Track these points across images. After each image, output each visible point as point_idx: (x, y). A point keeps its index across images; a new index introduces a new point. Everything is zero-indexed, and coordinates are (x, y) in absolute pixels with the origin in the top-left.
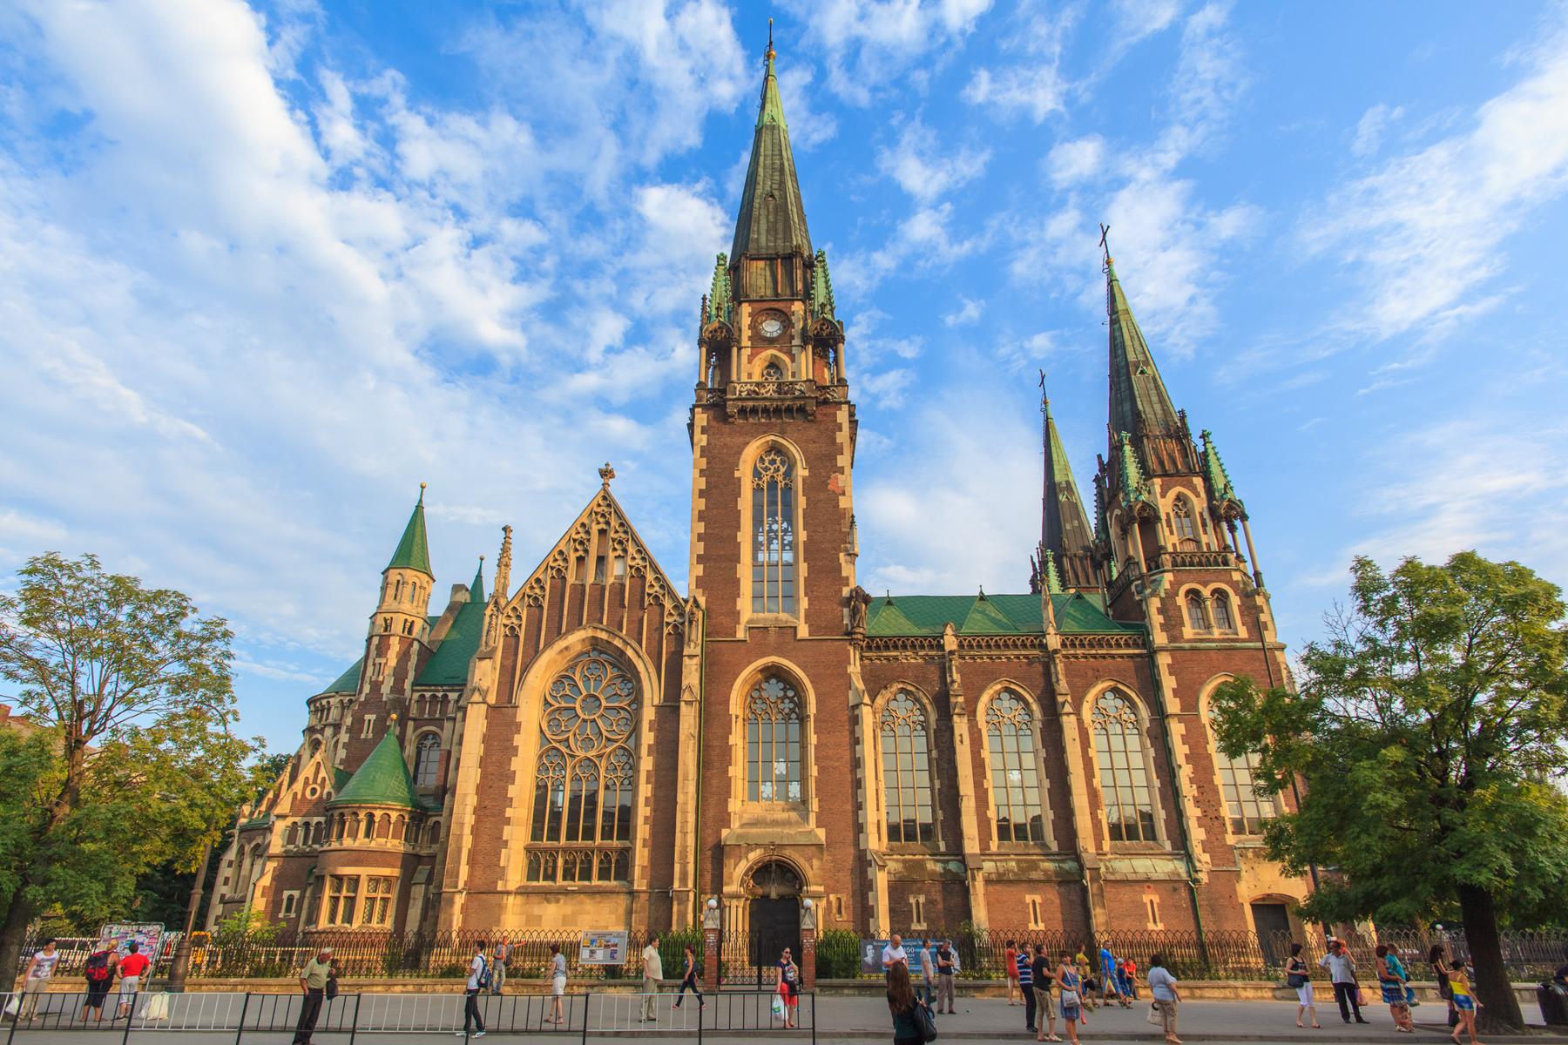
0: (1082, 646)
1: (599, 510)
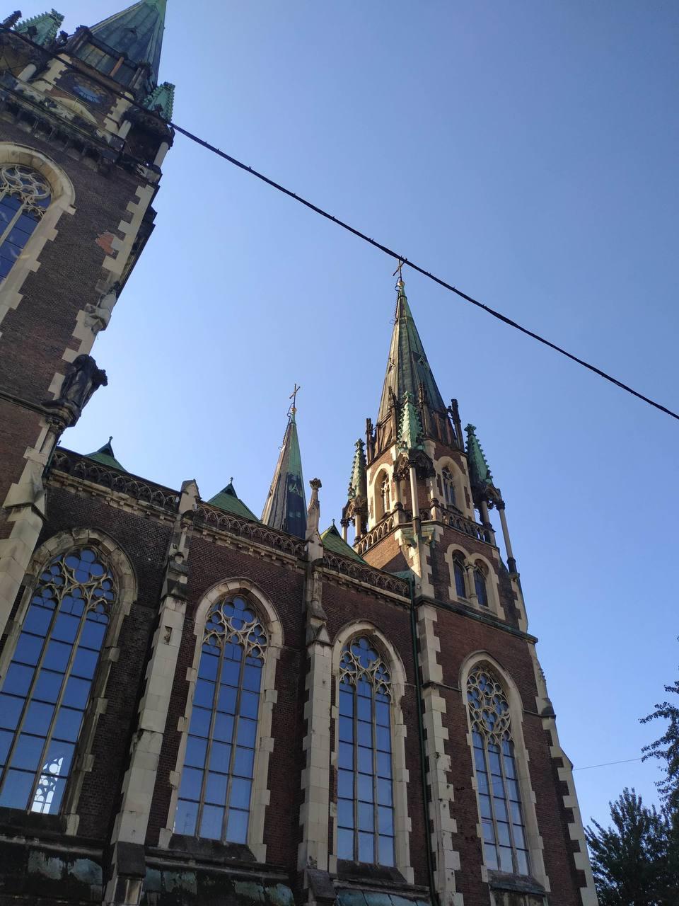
0: (343, 570)
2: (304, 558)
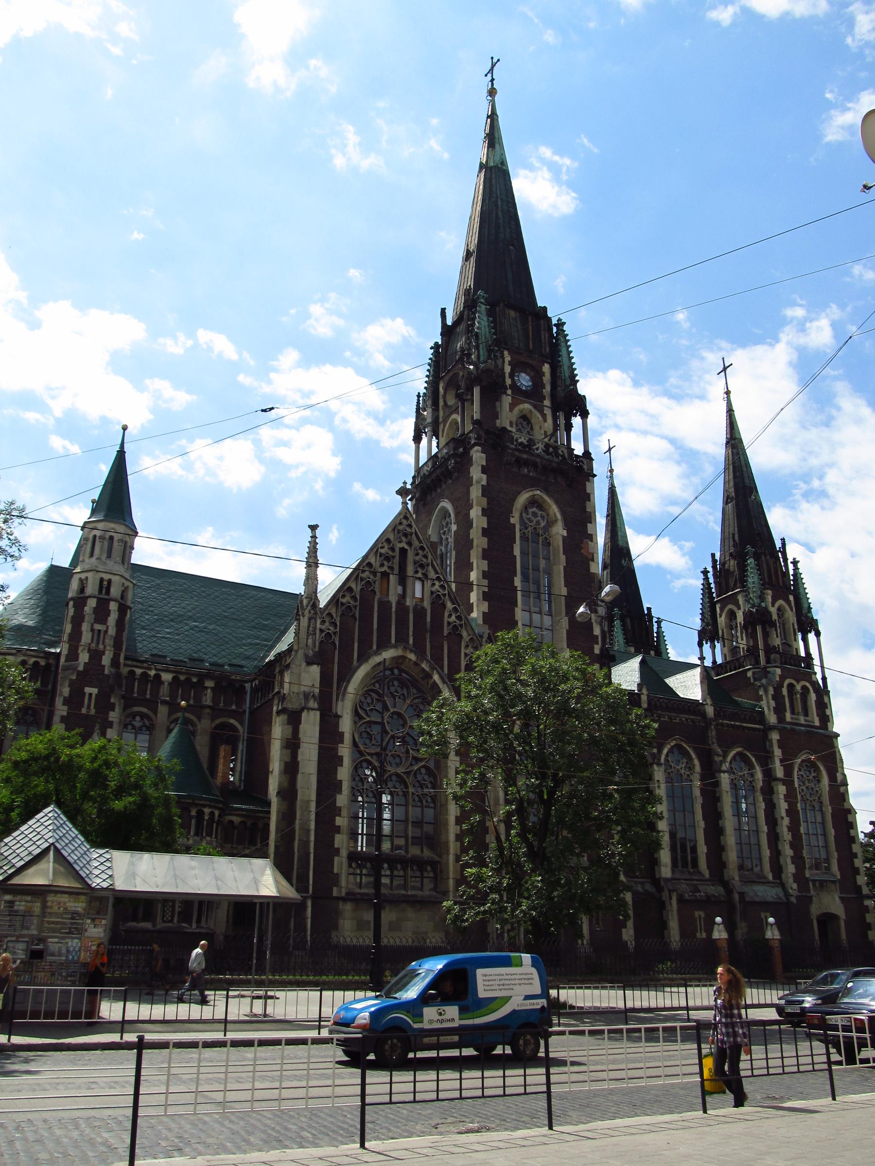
1: (401, 528)
2: (703, 714)
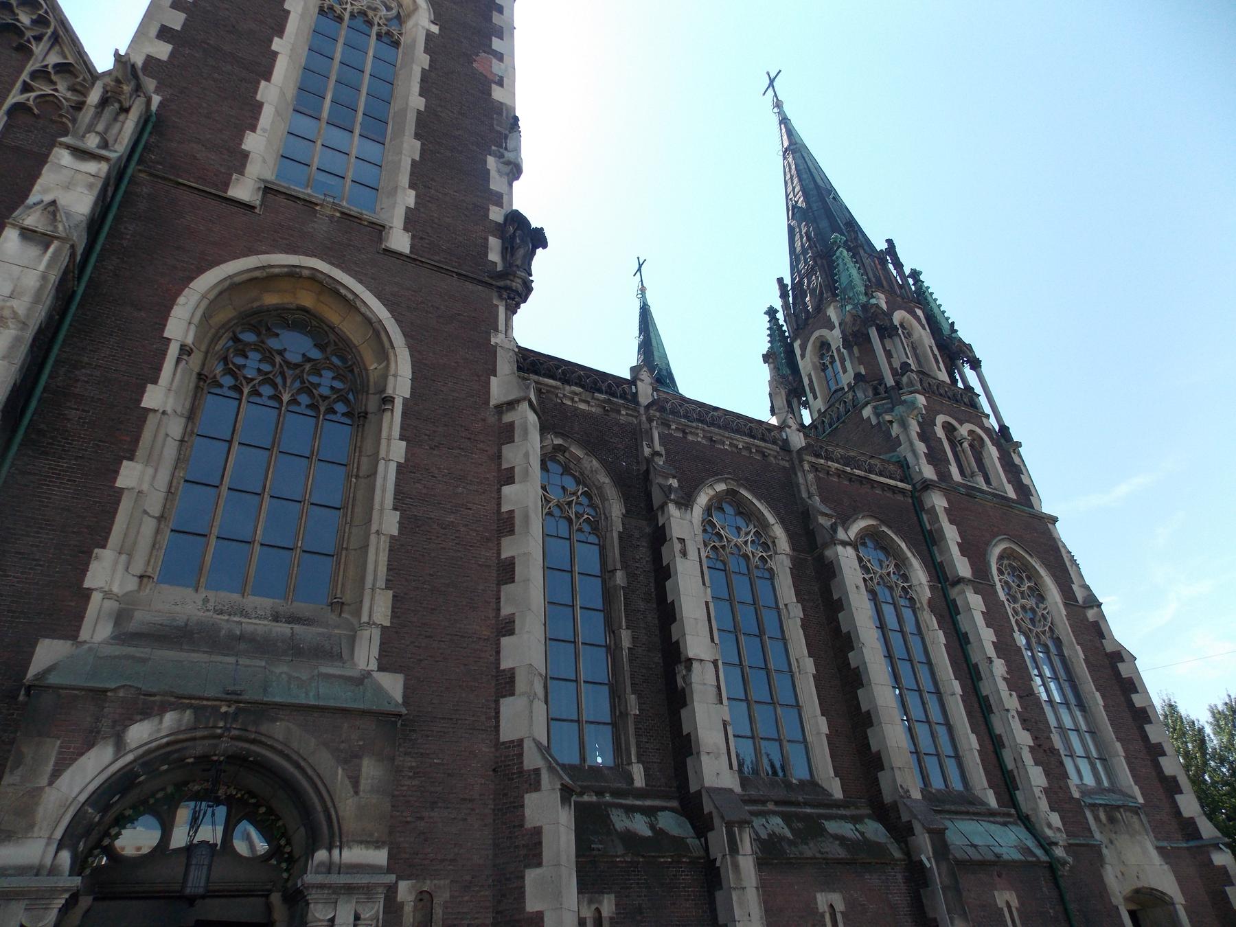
2: (785, 446)
